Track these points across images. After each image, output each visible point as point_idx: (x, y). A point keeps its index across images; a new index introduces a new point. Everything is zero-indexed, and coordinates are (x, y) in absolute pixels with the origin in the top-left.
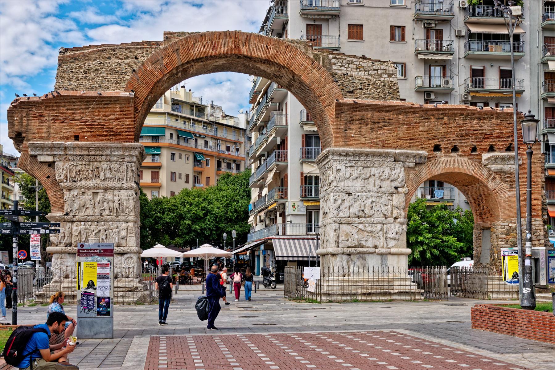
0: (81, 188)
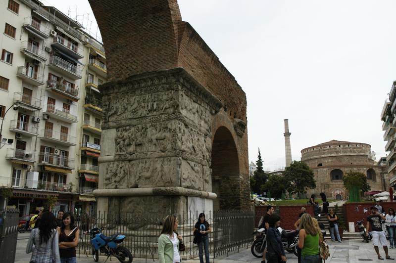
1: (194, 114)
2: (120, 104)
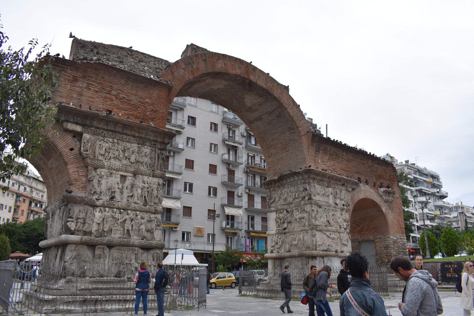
0: (110, 168)
1: (328, 196)
2: (277, 194)
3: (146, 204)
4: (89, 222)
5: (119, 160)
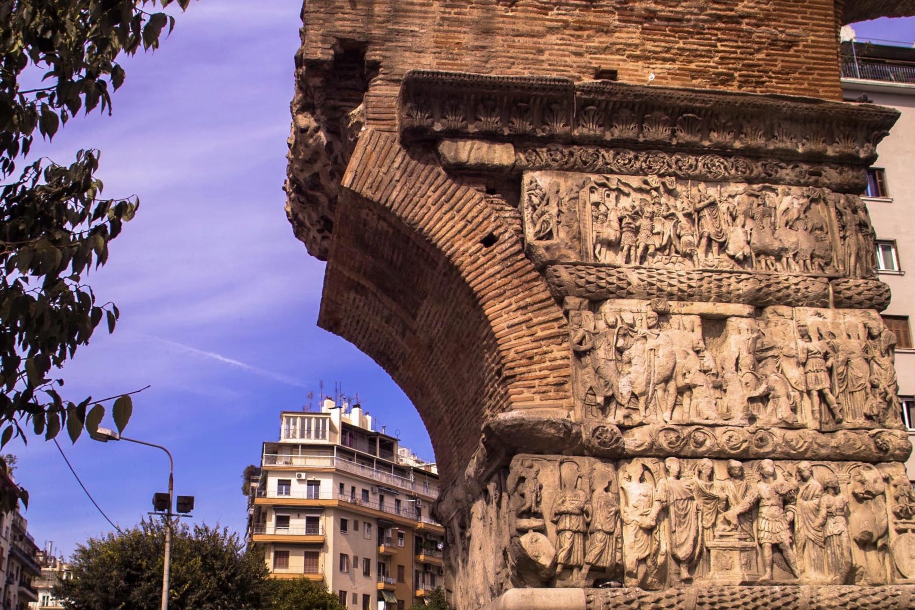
0: (650, 292)
3: (831, 426)
4: (608, 528)
5: (685, 255)
